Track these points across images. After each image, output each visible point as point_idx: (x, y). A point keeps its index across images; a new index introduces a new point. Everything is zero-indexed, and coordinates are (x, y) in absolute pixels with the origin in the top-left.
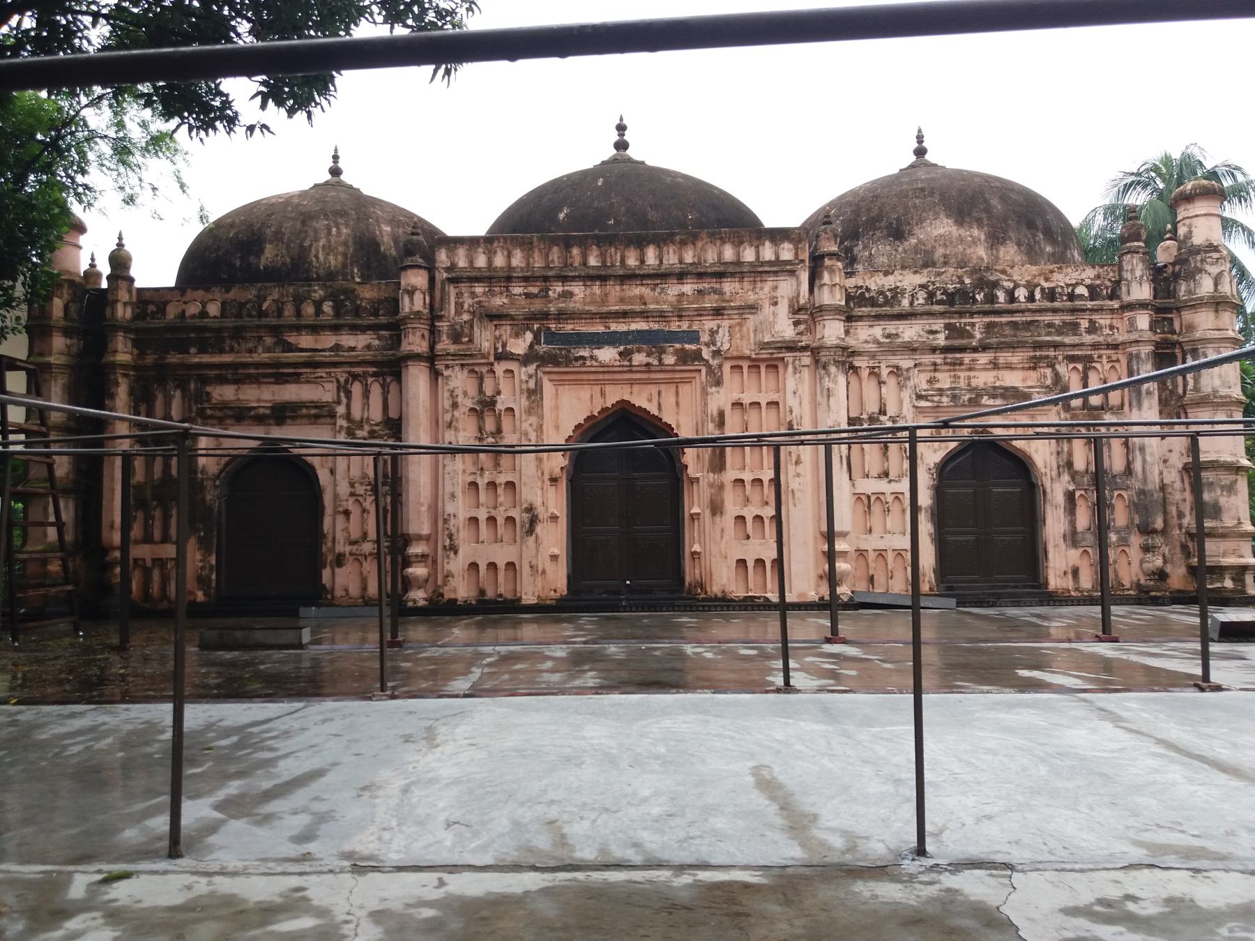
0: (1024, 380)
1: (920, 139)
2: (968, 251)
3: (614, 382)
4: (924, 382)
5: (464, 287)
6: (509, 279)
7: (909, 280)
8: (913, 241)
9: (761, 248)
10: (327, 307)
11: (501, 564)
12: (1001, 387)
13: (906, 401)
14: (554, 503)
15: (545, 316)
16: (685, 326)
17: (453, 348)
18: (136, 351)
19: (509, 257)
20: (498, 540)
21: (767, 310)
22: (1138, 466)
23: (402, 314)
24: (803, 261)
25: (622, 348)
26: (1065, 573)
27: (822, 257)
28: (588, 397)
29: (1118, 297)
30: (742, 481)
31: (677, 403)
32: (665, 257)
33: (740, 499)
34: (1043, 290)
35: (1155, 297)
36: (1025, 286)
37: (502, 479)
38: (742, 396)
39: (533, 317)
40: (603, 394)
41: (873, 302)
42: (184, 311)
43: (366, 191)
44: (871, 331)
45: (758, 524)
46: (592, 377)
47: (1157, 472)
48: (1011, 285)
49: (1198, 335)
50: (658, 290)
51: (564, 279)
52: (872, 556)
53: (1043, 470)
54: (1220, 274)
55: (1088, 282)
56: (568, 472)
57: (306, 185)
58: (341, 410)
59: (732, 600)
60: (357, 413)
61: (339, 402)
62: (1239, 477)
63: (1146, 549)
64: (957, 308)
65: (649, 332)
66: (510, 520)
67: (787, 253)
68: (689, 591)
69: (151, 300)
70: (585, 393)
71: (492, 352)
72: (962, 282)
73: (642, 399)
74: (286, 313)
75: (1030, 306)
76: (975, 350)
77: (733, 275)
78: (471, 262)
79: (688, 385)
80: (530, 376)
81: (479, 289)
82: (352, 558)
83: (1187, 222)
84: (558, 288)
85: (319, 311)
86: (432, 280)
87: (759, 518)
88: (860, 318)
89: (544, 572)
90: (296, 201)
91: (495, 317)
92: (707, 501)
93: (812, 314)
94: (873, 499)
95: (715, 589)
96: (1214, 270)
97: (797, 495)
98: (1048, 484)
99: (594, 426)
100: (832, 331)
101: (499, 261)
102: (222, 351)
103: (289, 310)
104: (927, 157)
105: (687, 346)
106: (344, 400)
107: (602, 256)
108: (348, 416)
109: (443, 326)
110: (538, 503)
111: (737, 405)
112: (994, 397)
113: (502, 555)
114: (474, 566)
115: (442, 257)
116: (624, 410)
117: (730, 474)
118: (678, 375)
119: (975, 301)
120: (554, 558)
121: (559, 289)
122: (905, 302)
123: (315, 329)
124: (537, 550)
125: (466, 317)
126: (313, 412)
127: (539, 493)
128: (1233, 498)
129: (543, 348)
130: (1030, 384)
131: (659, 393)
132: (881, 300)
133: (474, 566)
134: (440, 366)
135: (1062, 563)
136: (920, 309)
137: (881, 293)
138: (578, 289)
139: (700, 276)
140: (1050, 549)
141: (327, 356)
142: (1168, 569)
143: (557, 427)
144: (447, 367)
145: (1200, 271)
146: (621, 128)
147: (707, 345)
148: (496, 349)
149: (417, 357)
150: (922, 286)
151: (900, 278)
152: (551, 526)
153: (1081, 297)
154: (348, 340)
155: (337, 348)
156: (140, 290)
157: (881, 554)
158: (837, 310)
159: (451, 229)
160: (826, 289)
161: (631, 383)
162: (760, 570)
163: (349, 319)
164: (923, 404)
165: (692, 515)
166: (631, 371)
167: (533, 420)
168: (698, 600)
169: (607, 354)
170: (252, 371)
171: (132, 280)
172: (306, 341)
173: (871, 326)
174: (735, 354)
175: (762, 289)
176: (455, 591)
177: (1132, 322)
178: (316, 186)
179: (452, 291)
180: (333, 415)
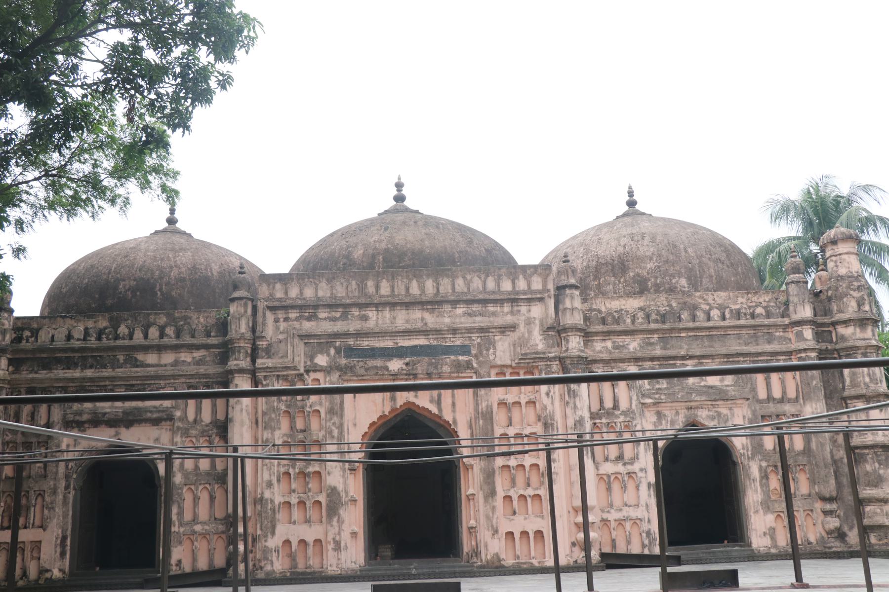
0: (722, 381)
1: (631, 193)
2: (674, 281)
5: (281, 315)
6: (316, 307)
7: (633, 304)
8: (632, 274)
9: (516, 281)
10: (170, 331)
11: (310, 540)
12: (705, 386)
13: (634, 398)
14: (353, 487)
15: (347, 335)
16: (458, 343)
17: (269, 363)
18: (11, 368)
19: (316, 290)
20: (308, 521)
21: (522, 328)
22: (814, 445)
23: (228, 337)
24: (548, 291)
25: (408, 360)
26: (765, 534)
27: (564, 287)
29: (788, 316)
30: (508, 467)
31: (454, 404)
32: (441, 288)
33: (507, 483)
34: (731, 311)
35: (815, 315)
36: (717, 308)
38: (506, 397)
39: (337, 335)
40: (393, 399)
41: (603, 321)
42: (53, 336)
43: (196, 236)
44: (603, 345)
45: (522, 502)
47: (828, 449)
48: (707, 307)
49: (848, 344)
50: (436, 313)
51: (361, 306)
52: (613, 524)
53: (742, 451)
55: (764, 304)
57: (146, 232)
58: (178, 414)
59: (503, 566)
60: (191, 416)
61: (175, 408)
64: (666, 326)
65: (429, 347)
66: (319, 503)
67: (537, 284)
69: (25, 325)
70: (378, 397)
71: (302, 364)
72: (670, 305)
73: (423, 400)
74: (135, 336)
75: (722, 324)
76: (683, 358)
77: (495, 301)
78: (286, 293)
81: (293, 315)
82: (186, 537)
83: (834, 258)
84: (356, 312)
85: (162, 335)
86: (255, 308)
87: (522, 497)
89: (346, 548)
90: (143, 246)
91: (304, 337)
93: (559, 332)
94: (612, 477)
95: (486, 556)
98: (746, 462)
99: (385, 423)
100: (575, 344)
101: (309, 293)
102: (84, 367)
103: (138, 335)
104: (637, 207)
105: (461, 358)
106: (182, 406)
107: (392, 287)
108: (184, 418)
109: (262, 344)
110: (340, 488)
111: (502, 403)
112: (700, 394)
113: (310, 533)
114: (287, 542)
115: (264, 291)
116: (410, 409)
119: (680, 319)
120: (354, 535)
121: (357, 313)
122: (629, 321)
123: (160, 349)
125: (281, 337)
126: (155, 416)
127: (341, 480)
129: (344, 361)
130: (726, 383)
131: (439, 396)
132: (610, 319)
133: (287, 542)
134: (260, 375)
135: (761, 524)
136: (641, 328)
137: (611, 314)
138: (372, 313)
139: (469, 302)
140: (751, 513)
141: (170, 371)
142: (846, 529)
144: (265, 377)
145: (846, 295)
146: (399, 186)
147: (476, 356)
148: (305, 362)
149: (241, 371)
150: (641, 309)
151: (624, 302)
152: (351, 507)
153: (760, 315)
154: (186, 357)
155: (176, 363)
156: (18, 318)
157: (620, 522)
158: (576, 329)
159: (269, 268)
160: (568, 313)
162: (525, 540)
163: (187, 339)
165: (467, 496)
167: (336, 419)
169: (395, 365)
170: (107, 383)
171: (11, 311)
172: (151, 358)
174: (499, 363)
175: (519, 311)
176: (272, 563)
177: (800, 336)
178: (157, 232)
179: (270, 317)
180: (171, 418)
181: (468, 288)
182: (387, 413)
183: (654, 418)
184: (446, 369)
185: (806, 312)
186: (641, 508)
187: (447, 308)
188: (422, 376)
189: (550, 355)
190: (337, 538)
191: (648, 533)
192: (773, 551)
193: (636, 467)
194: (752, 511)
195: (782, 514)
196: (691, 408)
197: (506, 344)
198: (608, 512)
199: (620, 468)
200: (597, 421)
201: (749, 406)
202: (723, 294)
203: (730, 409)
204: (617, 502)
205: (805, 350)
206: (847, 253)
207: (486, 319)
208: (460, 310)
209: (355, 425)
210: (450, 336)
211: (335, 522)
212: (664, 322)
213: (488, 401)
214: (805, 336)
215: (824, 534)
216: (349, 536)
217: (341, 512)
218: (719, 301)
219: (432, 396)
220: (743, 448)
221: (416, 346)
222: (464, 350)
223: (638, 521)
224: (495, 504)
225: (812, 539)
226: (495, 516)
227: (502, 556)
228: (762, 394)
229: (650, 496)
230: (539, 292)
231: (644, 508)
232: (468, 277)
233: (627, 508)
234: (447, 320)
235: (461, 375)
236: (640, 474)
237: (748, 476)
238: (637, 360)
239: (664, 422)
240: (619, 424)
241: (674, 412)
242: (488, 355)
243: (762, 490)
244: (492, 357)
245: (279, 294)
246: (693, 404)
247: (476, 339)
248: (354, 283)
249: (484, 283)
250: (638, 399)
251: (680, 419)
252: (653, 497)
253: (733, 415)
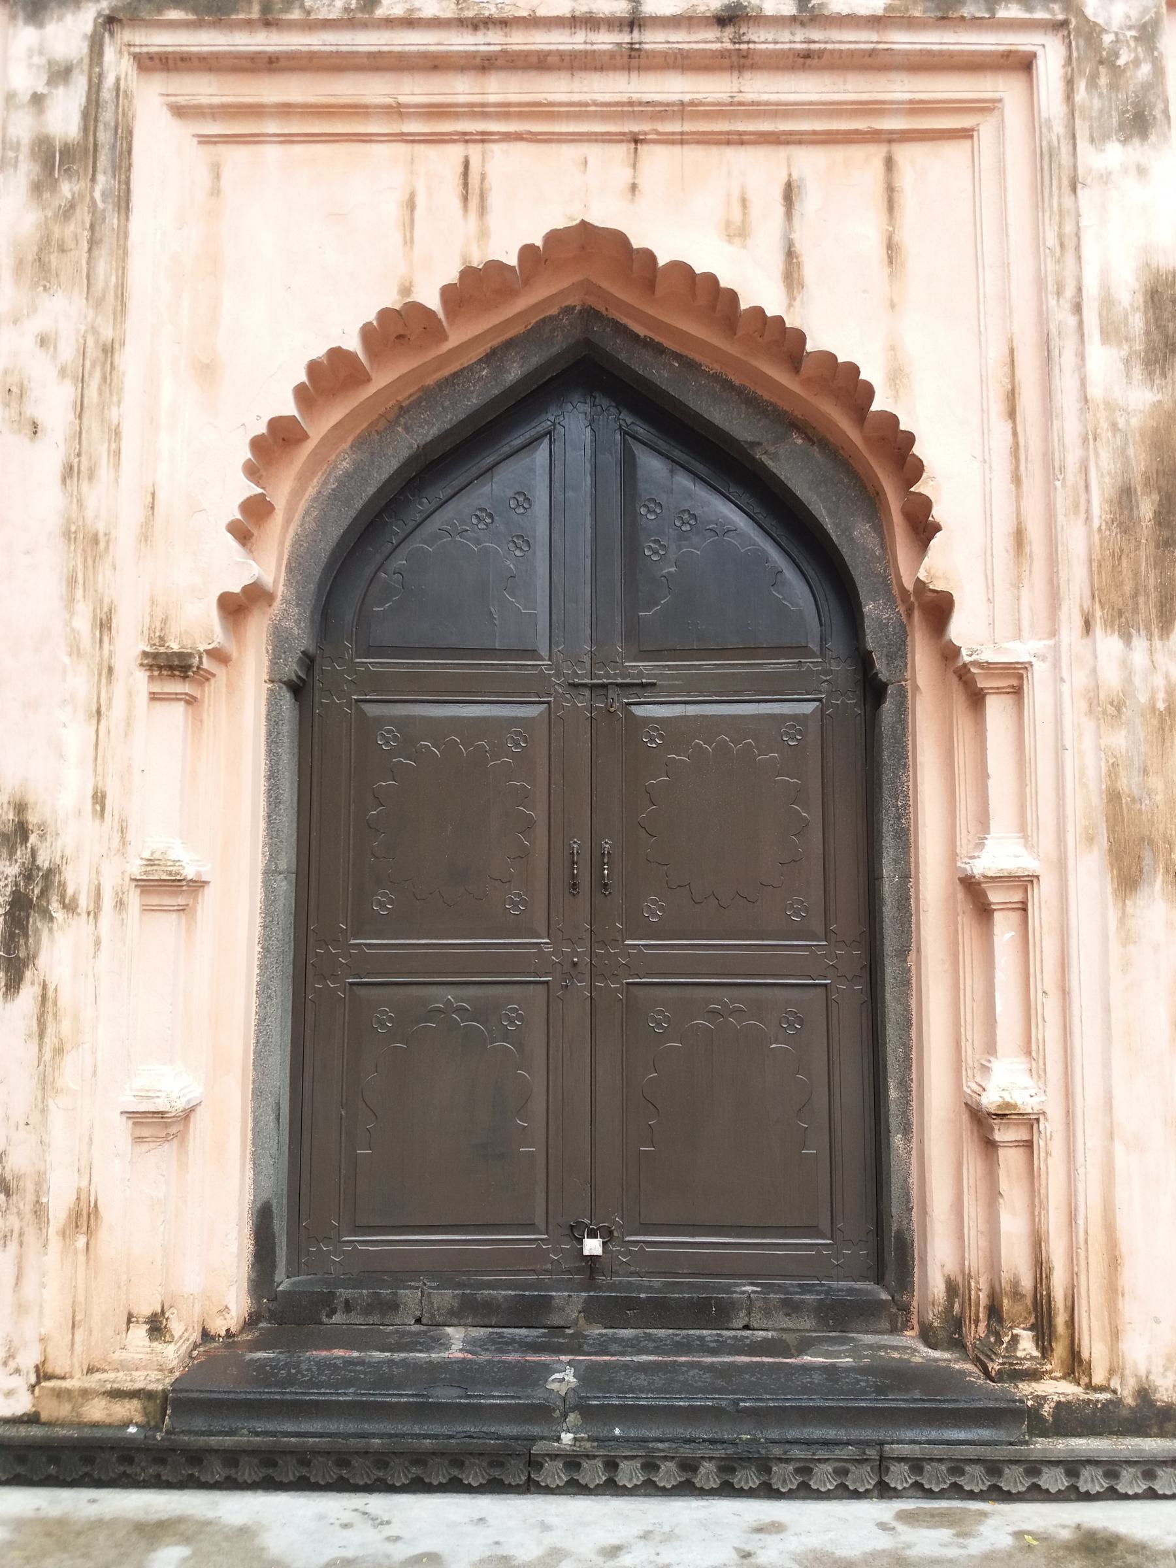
3: (536, 125)
28: (392, 207)
31: (892, 249)
46: (415, 90)
56: (279, 641)
68: (950, 1332)
79: (954, 153)
80: (60, 74)
89: (85, 1218)
92: (1084, 803)
118: (900, 88)
124: (46, 1084)
127: (76, 735)
131: (790, 195)
143: (207, 371)
161: (635, 129)
166: (633, 60)
168: (1030, 1419)
188: (681, 39)
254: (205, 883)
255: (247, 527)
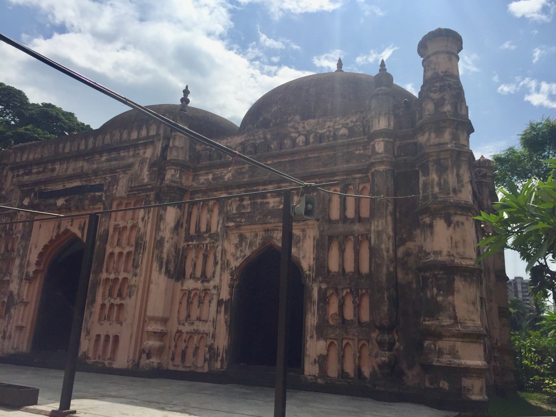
4: (234, 208)
8: (261, 119)
13: (221, 221)
16: (97, 183)
21: (136, 167)
26: (315, 361)
32: (97, 142)
37: (6, 279)
40: (59, 227)
51: (53, 162)
53: (308, 273)
54: (443, 99)
55: (351, 125)
62: (455, 277)
63: (381, 344)
72: (265, 138)
76: (265, 183)
87: (112, 305)
88: (201, 169)
96: (436, 96)
97: (134, 289)
105: (97, 194)
110: (15, 292)
111: (116, 228)
117: (104, 275)
120: (20, 328)
121: (50, 167)
127: (17, 287)
128: (450, 298)
147: (106, 192)
150: (242, 144)
151: (230, 140)
157: (190, 334)
164: (231, 224)
167: (23, 243)
169: (60, 202)
173: (207, 174)
174: (118, 195)
175: (138, 154)
181: (112, 141)
182: (54, 238)
183: (236, 241)
184: (87, 202)
185: (382, 124)
186: (208, 323)
187: (97, 157)
189: (149, 187)
190: (5, 330)
191: (211, 348)
192: (320, 381)
193: (212, 284)
194: (309, 335)
195: (335, 342)
196: (268, 230)
197: (125, 181)
198: (183, 324)
199: (199, 285)
200: (190, 243)
201: (319, 228)
202: (312, 121)
203: (303, 230)
204: (194, 317)
205: (372, 164)
206: (436, 53)
207: (117, 162)
208: (103, 159)
209: (36, 247)
210: (94, 178)
211: (7, 319)
212: (256, 153)
213: (105, 225)
214: (377, 150)
215: (377, 368)
216: (14, 328)
217: (12, 311)
218: (308, 128)
219: (80, 225)
220: (310, 270)
221: (74, 187)
222: (99, 188)
223: (205, 335)
224: (93, 310)
225: (366, 372)
226: (91, 320)
227: (90, 355)
228: (335, 214)
229: (218, 312)
230: (153, 137)
231: (211, 323)
232: (114, 132)
233: (197, 323)
234: (95, 166)
235: (95, 207)
236: (214, 292)
237: (311, 297)
238: (227, 187)
239: (244, 244)
240: (205, 245)
241: (253, 234)
242: (113, 190)
243: (318, 314)
244: (114, 192)
245: (18, 160)
246: (268, 226)
247: (108, 177)
248: (53, 146)
249: (121, 135)
250: (223, 222)
251: (258, 241)
252: (223, 313)
253: (305, 236)
254: (28, 303)
255: (38, 263)
